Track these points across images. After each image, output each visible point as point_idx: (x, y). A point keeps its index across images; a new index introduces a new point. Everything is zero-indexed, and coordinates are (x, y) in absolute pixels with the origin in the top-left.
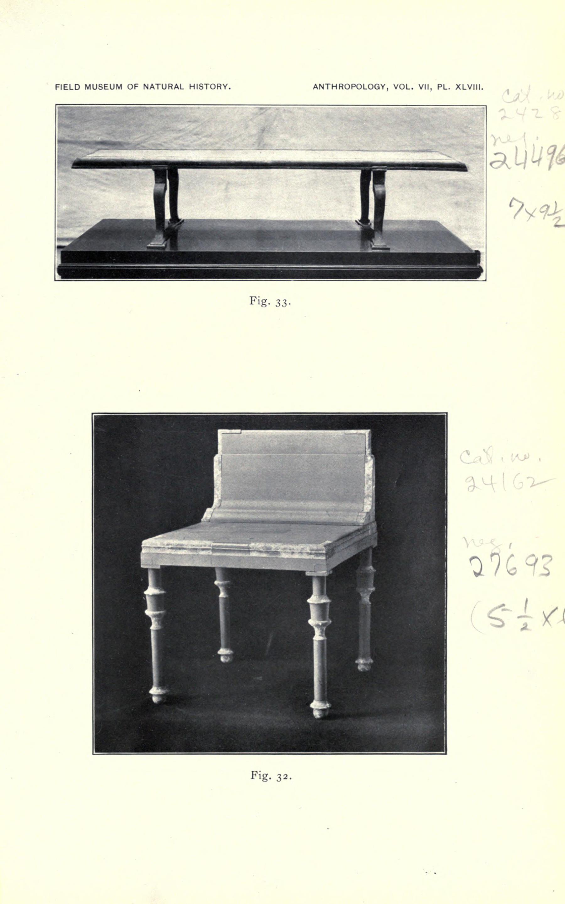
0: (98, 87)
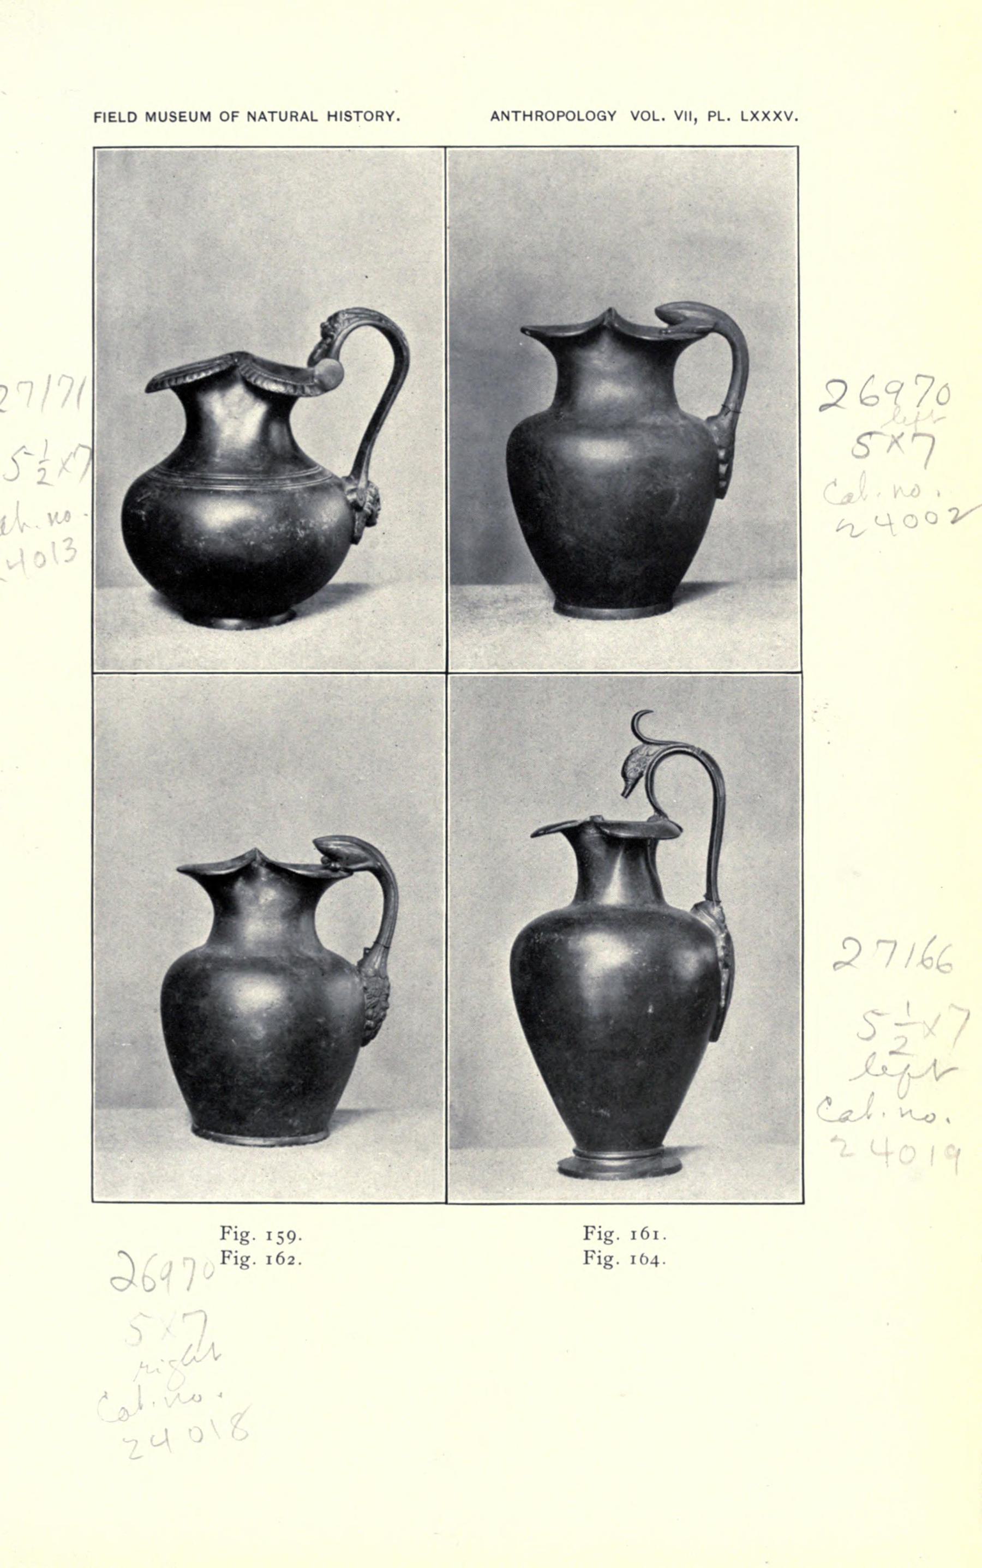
0: (169, 117)
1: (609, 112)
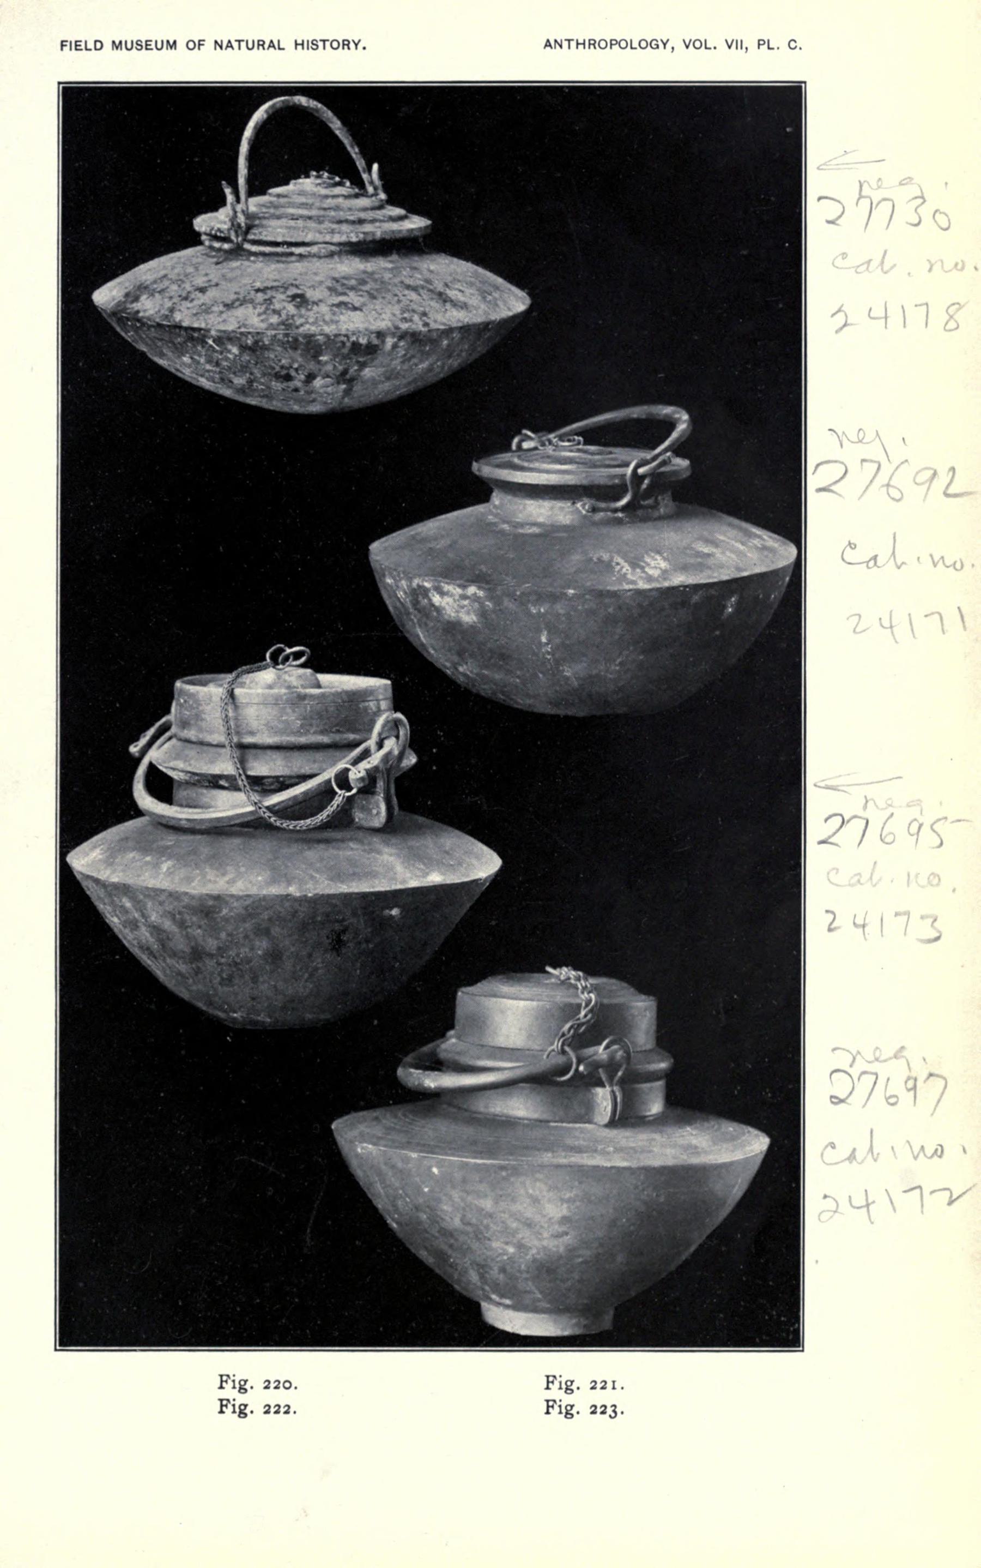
0: (135, 45)
1: (662, 41)
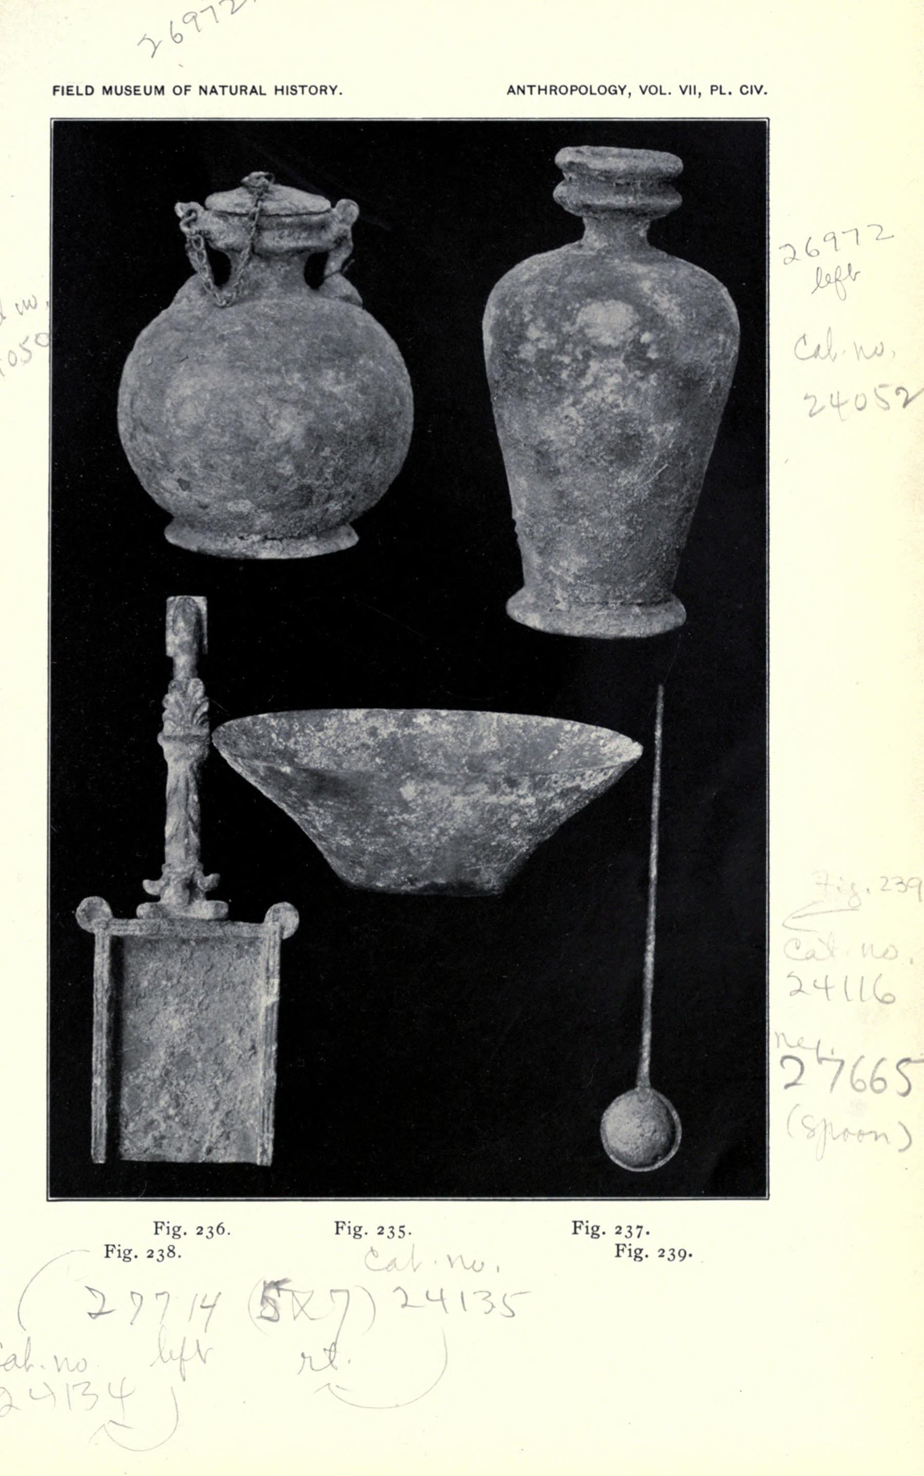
0: (124, 90)
1: (619, 87)
